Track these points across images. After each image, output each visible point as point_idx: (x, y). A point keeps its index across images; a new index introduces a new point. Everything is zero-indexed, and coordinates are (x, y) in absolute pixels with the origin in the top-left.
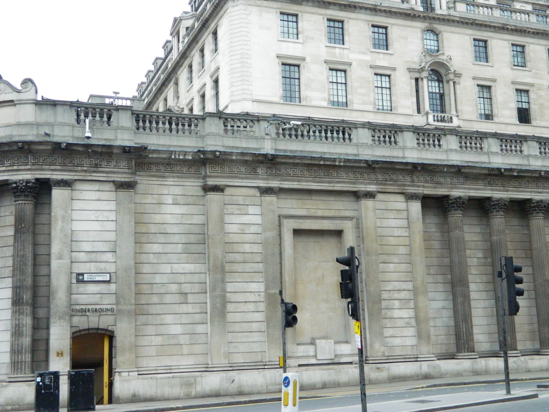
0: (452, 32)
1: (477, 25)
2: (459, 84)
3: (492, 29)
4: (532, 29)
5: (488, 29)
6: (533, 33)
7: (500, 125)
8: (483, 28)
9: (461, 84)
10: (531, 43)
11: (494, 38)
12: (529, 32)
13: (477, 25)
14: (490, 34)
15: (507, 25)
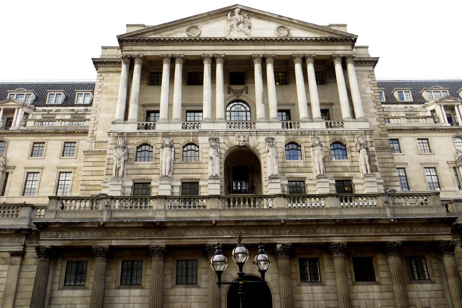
0: (16, 140)
1: (36, 133)
2: (12, 173)
3: (49, 135)
4: (80, 130)
5: (46, 134)
6: (82, 133)
7: (38, 198)
8: (42, 135)
9: (14, 174)
10: (81, 140)
11: (50, 140)
12: (78, 132)
13: (36, 133)
14: (48, 138)
15: (59, 130)
